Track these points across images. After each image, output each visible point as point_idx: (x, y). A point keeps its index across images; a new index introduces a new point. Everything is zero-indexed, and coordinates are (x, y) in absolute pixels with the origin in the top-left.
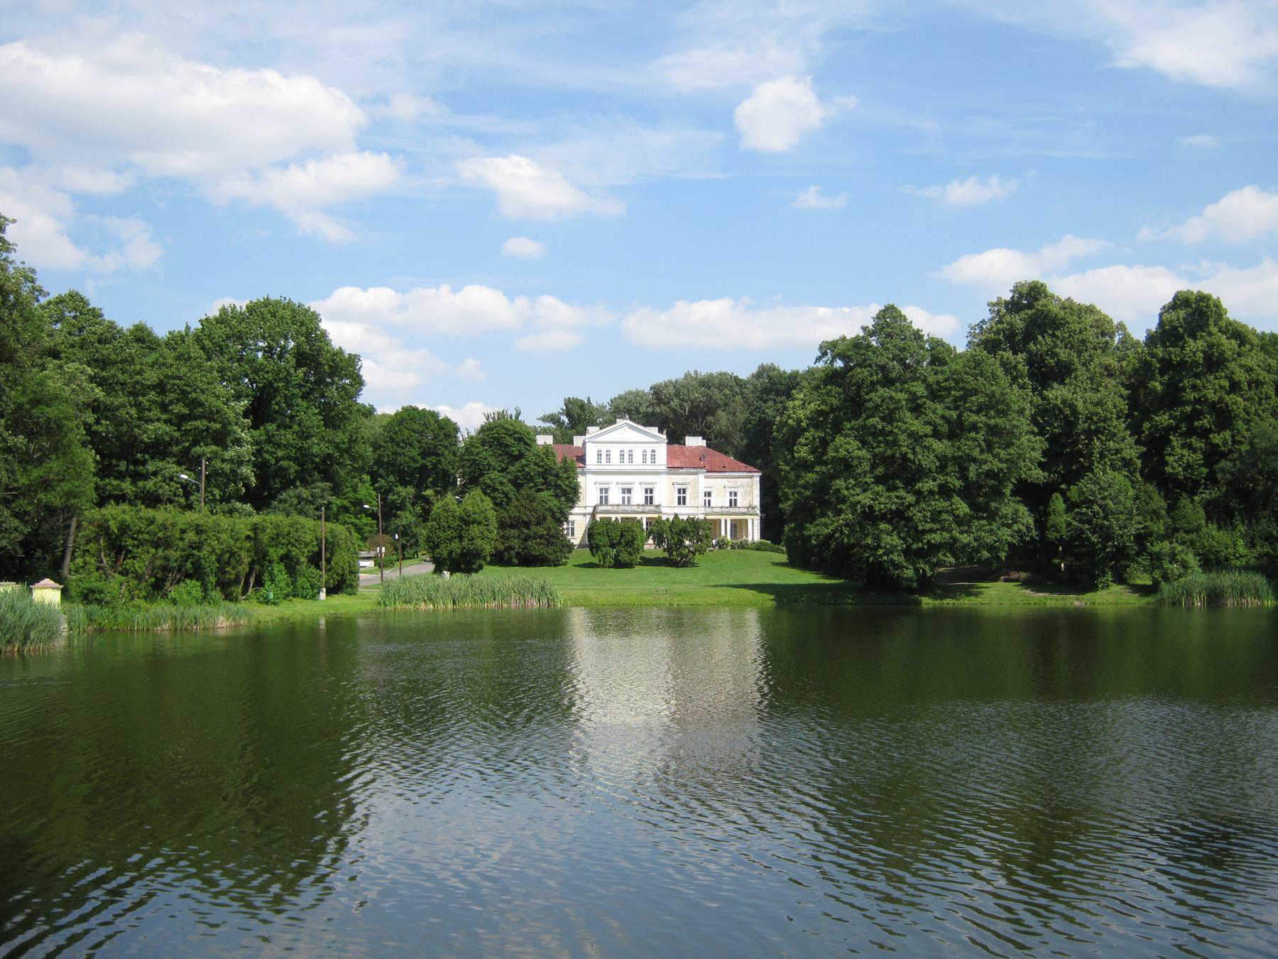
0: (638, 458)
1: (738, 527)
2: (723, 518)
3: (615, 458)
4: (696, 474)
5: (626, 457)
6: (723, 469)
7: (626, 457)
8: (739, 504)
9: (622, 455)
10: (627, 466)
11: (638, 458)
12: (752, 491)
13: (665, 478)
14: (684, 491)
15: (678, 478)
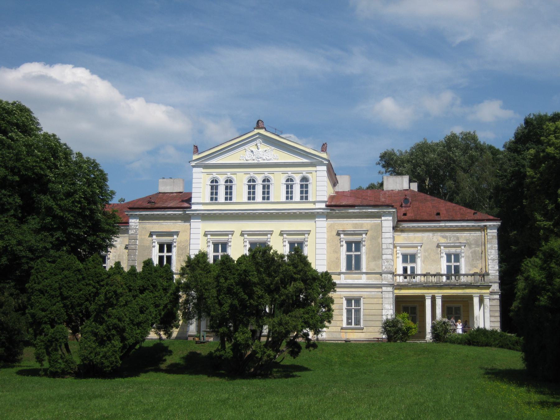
0: (278, 192)
1: (458, 308)
2: (427, 293)
3: (240, 192)
4: (378, 216)
5: (259, 190)
6: (437, 217)
7: (259, 190)
8: (463, 271)
9: (252, 188)
10: (259, 206)
11: (278, 192)
12: (484, 252)
13: (322, 224)
14: (358, 245)
15: (348, 224)
